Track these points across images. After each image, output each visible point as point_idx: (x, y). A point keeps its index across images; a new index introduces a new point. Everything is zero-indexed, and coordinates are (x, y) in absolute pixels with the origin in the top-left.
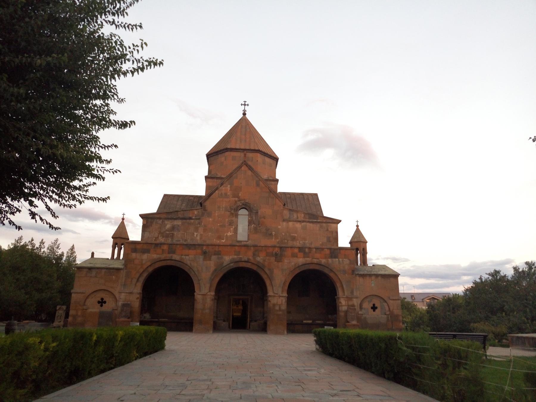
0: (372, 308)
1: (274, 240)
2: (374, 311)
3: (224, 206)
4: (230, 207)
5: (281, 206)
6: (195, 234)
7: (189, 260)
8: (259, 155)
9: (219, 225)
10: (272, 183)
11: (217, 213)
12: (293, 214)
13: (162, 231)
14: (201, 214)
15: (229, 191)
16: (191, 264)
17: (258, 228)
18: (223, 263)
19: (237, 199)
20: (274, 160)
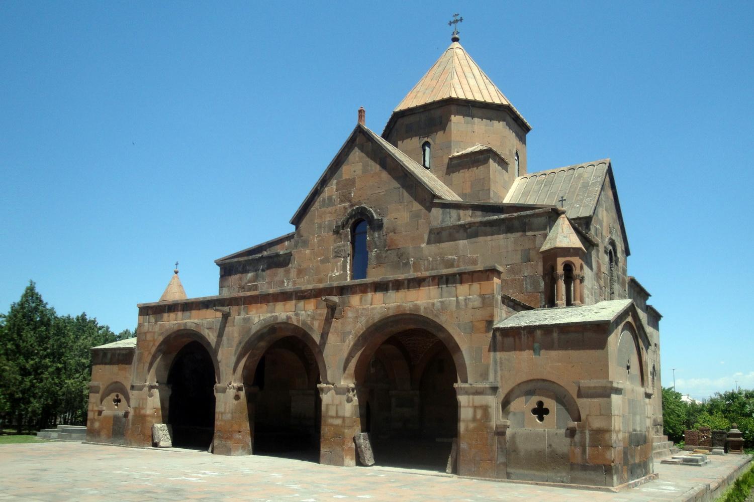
0: (535, 411)
1: (411, 273)
2: (541, 419)
3: (327, 223)
4: (336, 222)
5: (425, 200)
6: (285, 281)
7: (207, 329)
8: (453, 108)
9: (319, 259)
10: (480, 156)
11: (317, 237)
12: (450, 211)
13: (243, 284)
14: (293, 243)
15: (335, 190)
16: (209, 335)
17: (384, 255)
18: (250, 329)
19: (347, 204)
20: (499, 110)
